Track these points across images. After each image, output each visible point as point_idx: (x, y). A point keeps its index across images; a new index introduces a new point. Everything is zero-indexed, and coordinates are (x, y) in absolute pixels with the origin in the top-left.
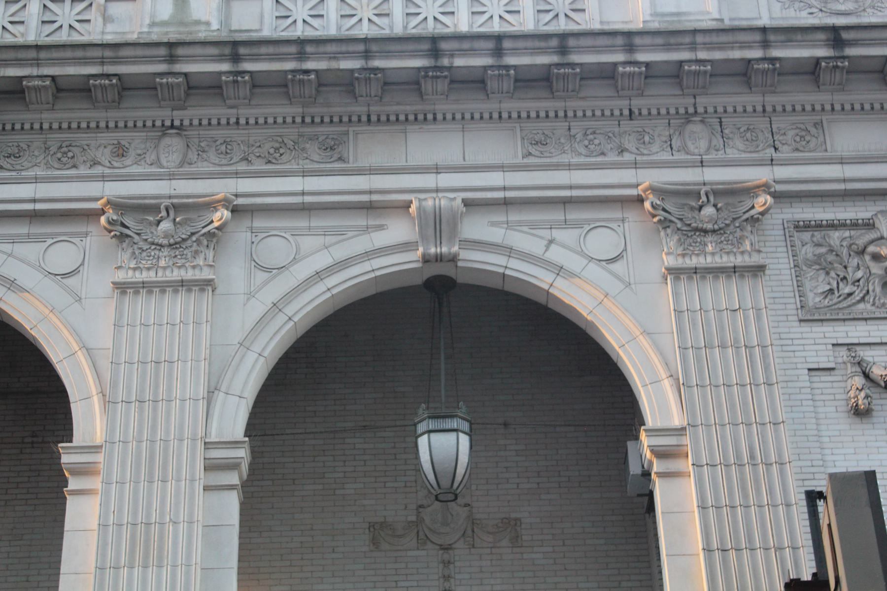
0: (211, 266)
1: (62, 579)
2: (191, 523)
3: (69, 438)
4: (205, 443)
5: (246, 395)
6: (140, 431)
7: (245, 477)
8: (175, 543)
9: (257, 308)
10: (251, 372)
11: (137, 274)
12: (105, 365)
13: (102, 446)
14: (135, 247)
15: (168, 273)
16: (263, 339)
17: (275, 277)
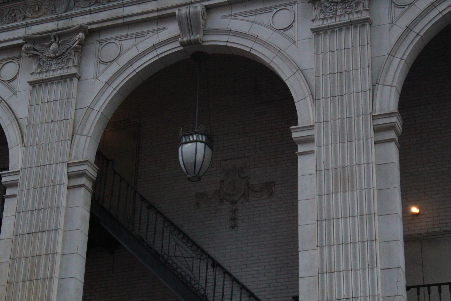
0: (367, 10)
1: (300, 203)
2: (368, 164)
3: (296, 122)
4: (373, 116)
5: (395, 84)
6: (335, 114)
7: (400, 132)
8: (360, 177)
9: (398, 31)
10: (397, 69)
11: (325, 22)
12: (311, 78)
13: (313, 126)
14: (323, 6)
15: (342, 18)
16: (402, 49)
17: (406, 11)
